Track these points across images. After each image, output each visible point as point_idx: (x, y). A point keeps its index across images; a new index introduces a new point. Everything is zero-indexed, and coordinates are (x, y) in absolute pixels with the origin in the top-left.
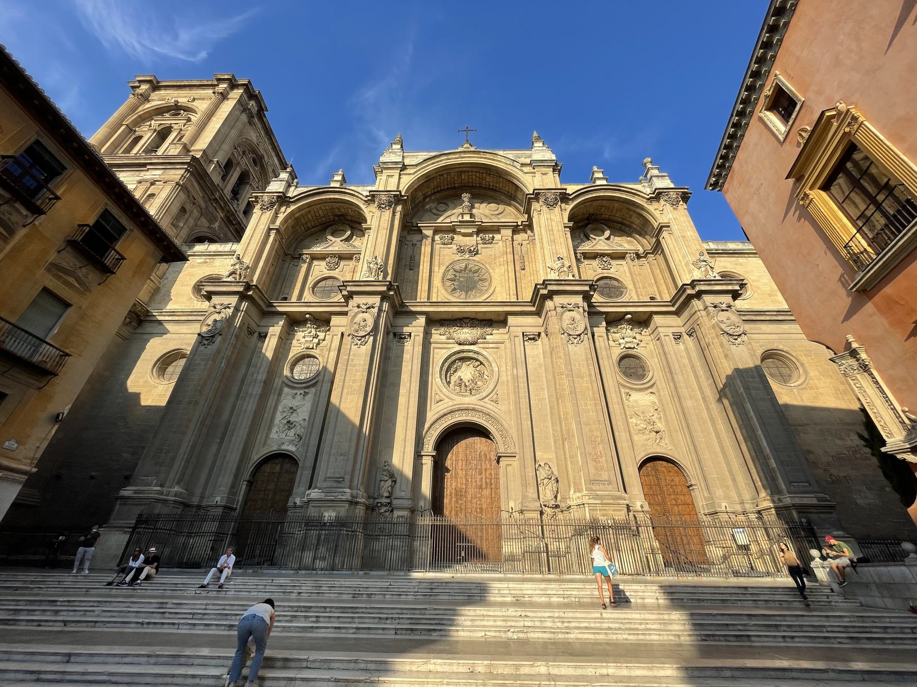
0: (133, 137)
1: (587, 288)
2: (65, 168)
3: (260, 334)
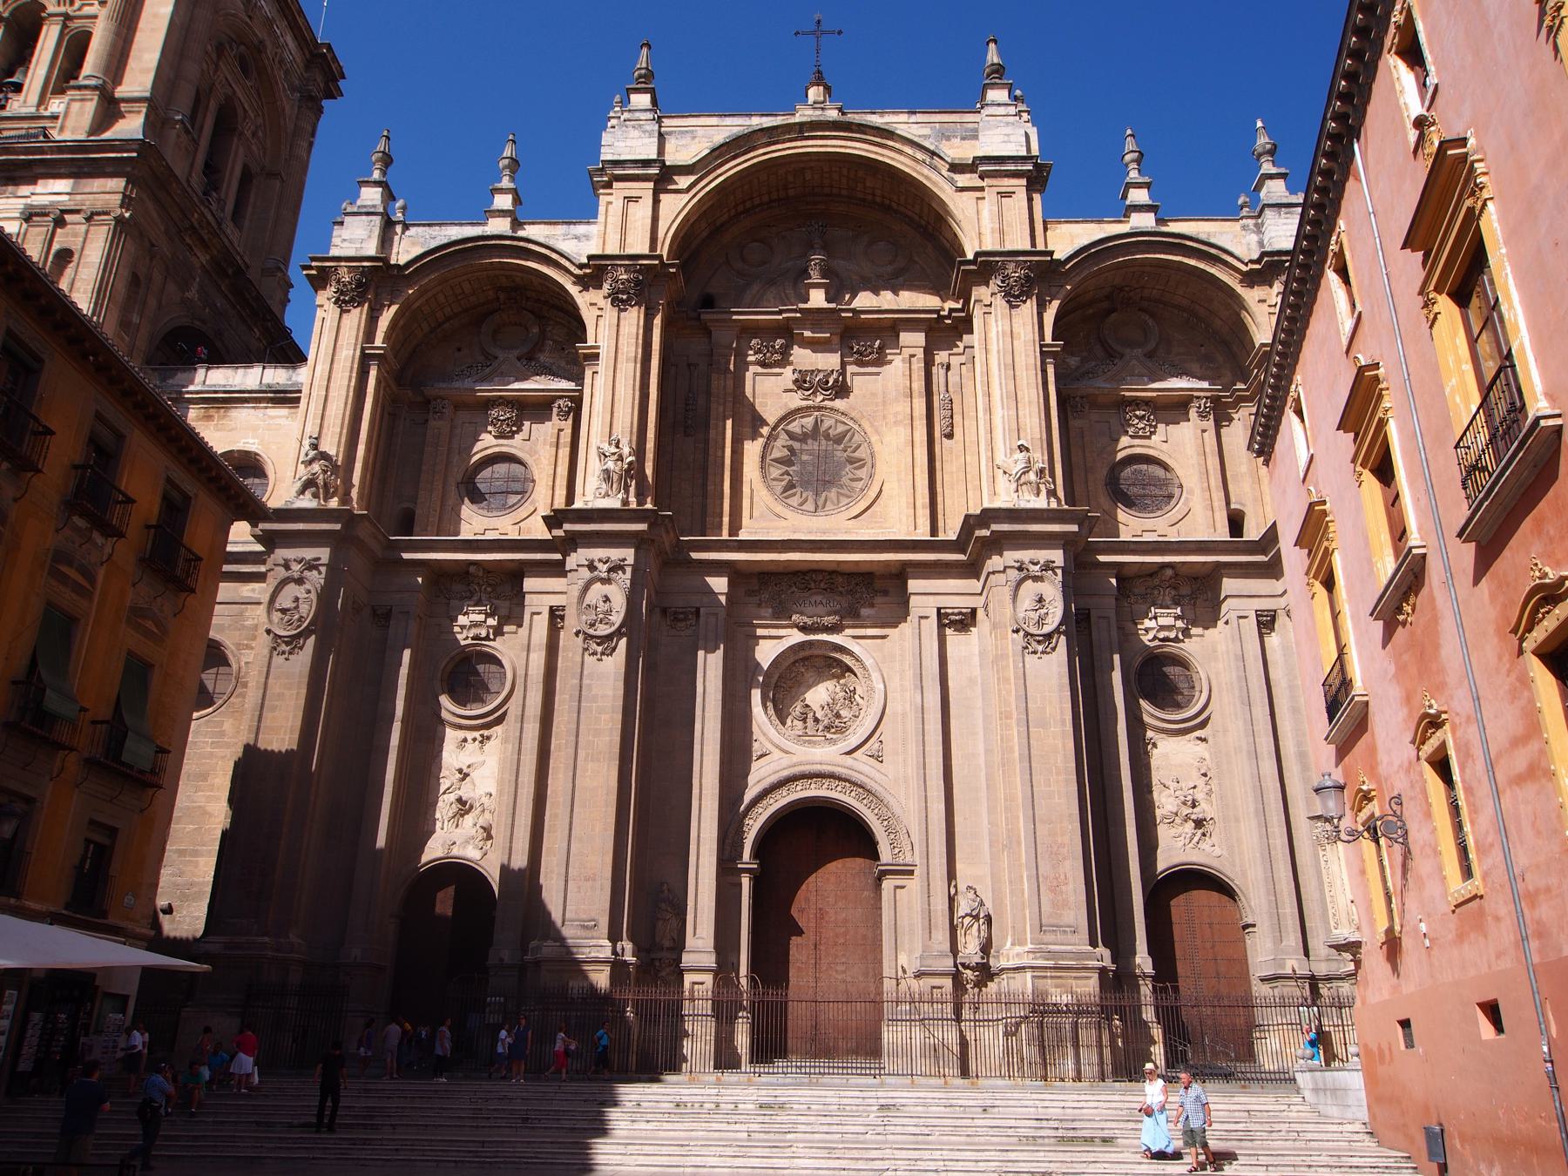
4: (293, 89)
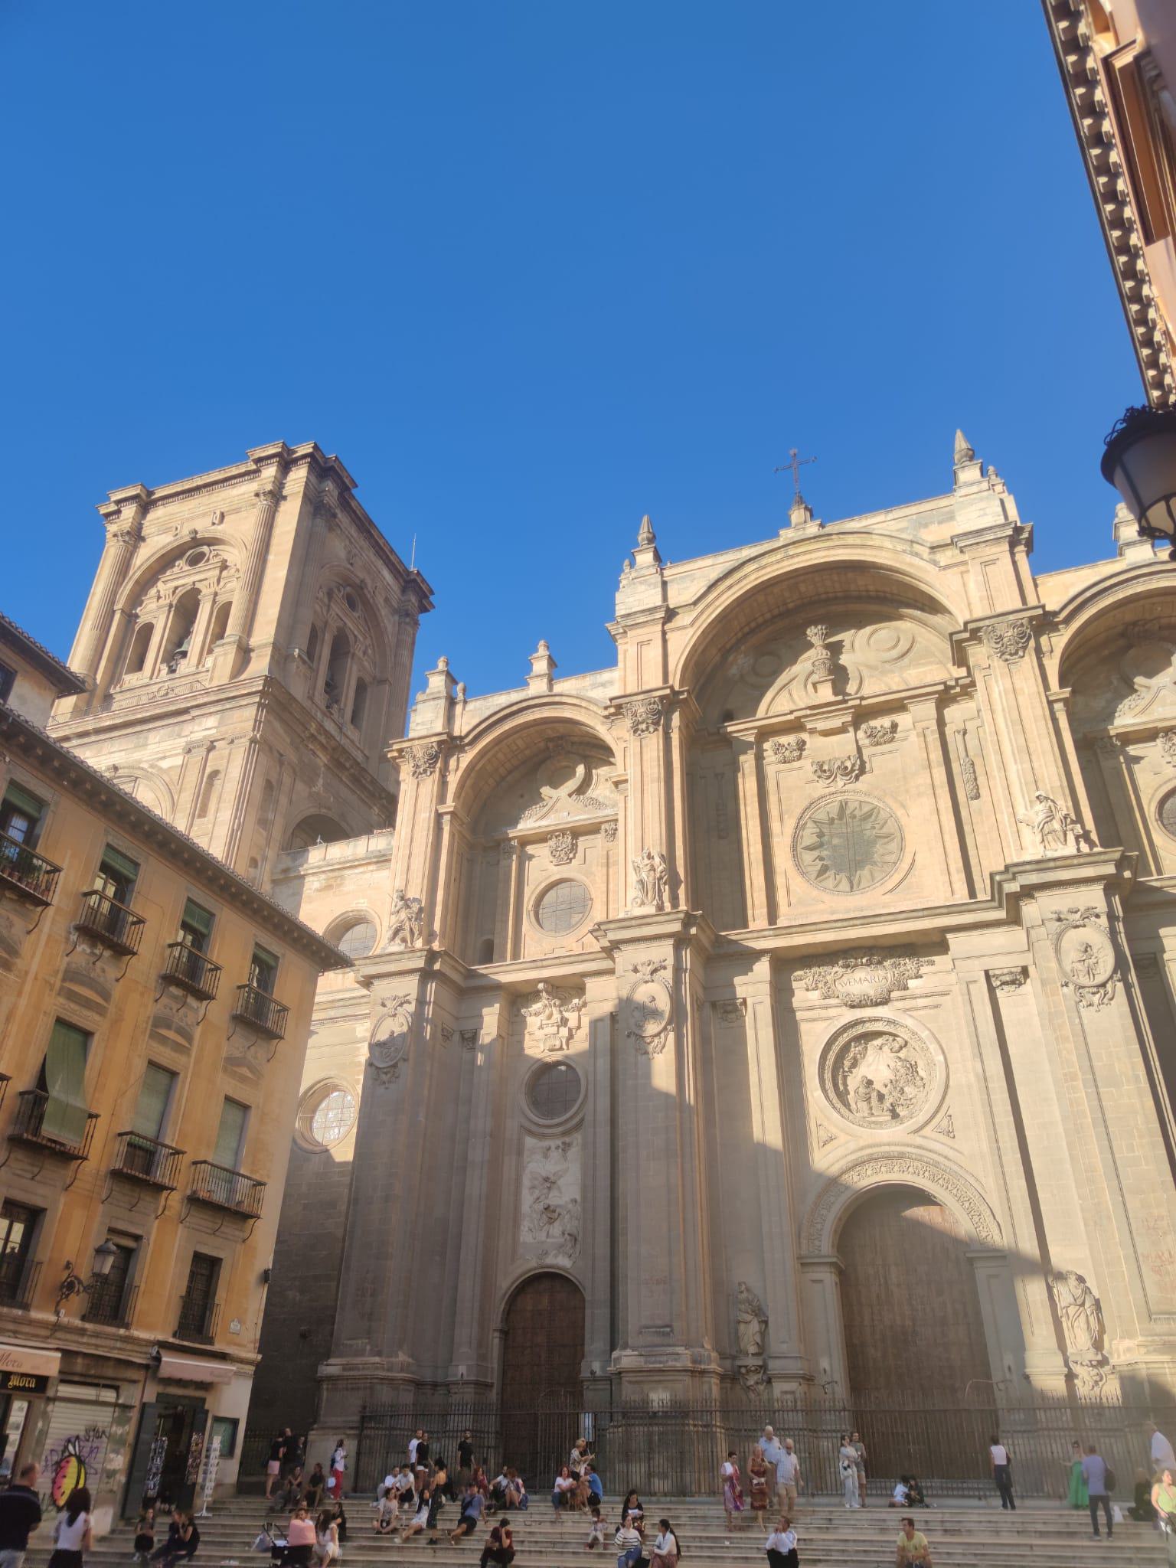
0: (137, 628)
1: (1110, 869)
2: (213, 915)
3: (462, 1034)
4: (395, 611)
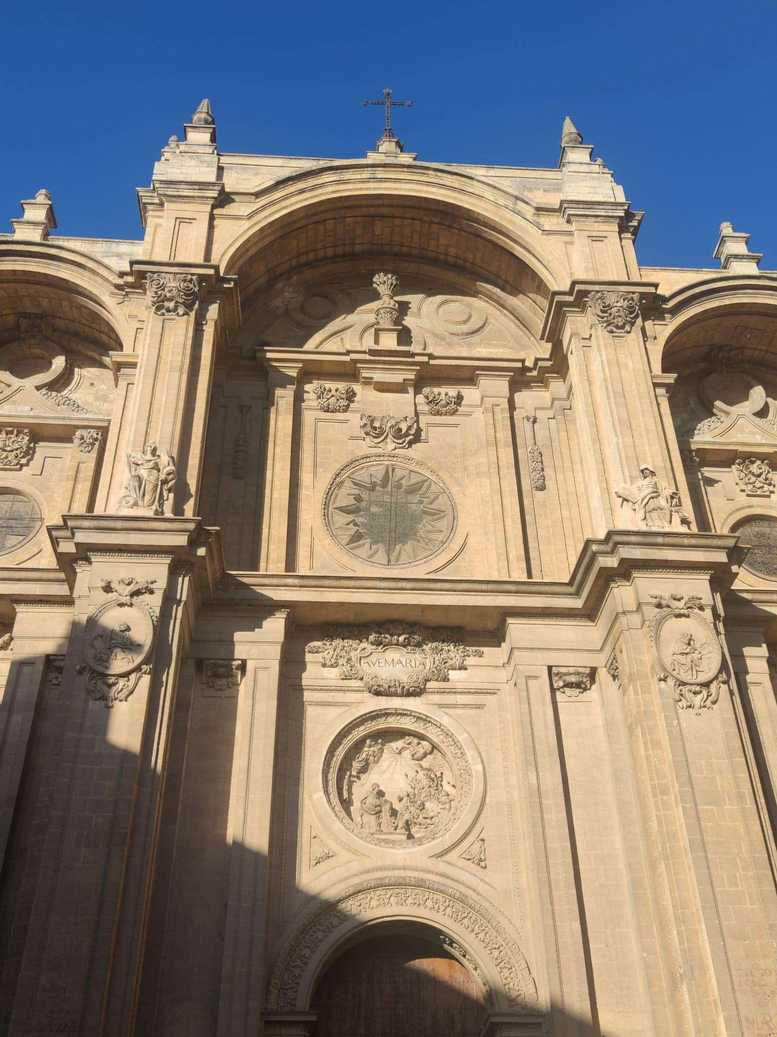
1: (722, 557)
